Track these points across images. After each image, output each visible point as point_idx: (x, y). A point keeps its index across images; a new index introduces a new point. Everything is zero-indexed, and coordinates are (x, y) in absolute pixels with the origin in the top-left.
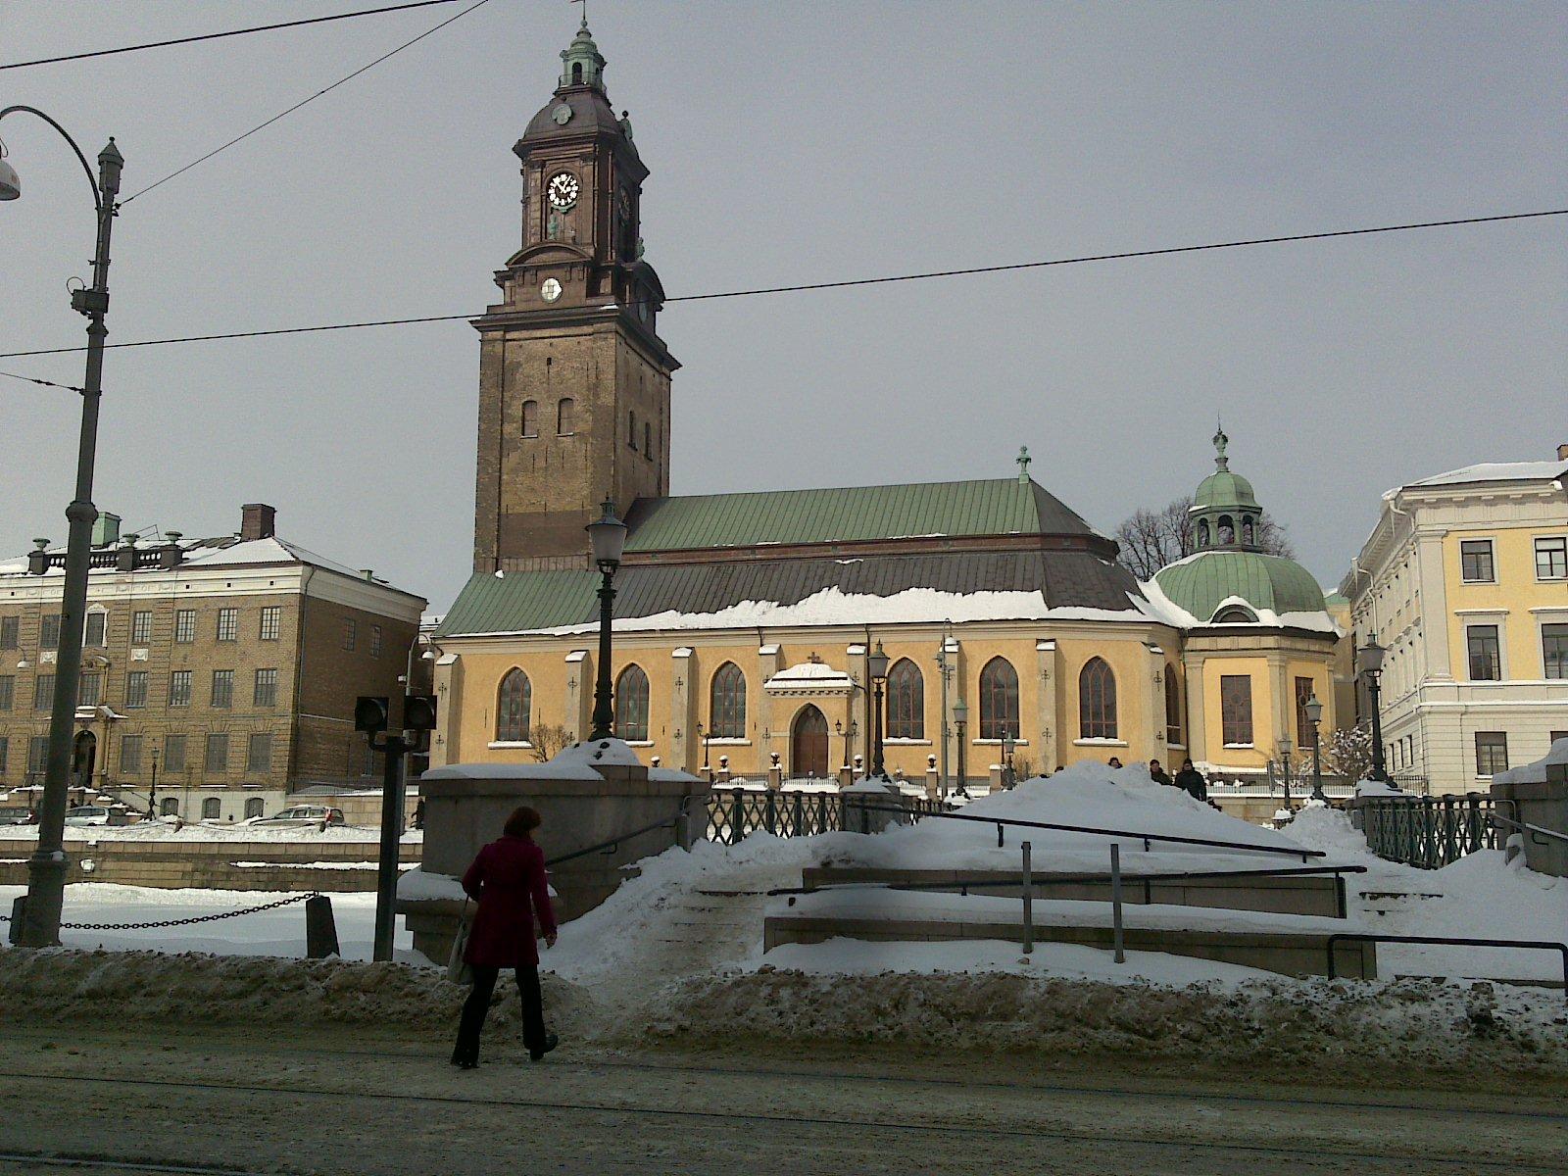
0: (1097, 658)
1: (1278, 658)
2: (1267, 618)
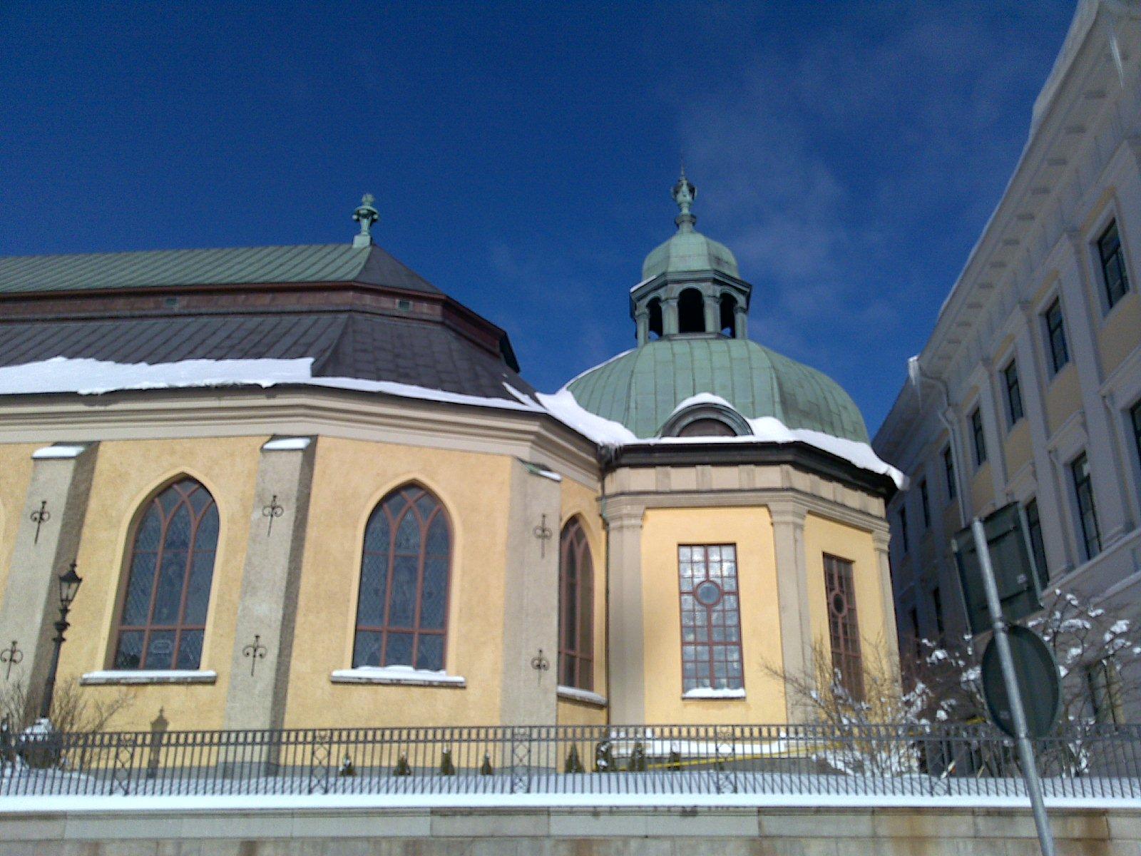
0: (413, 485)
1: (790, 506)
2: (768, 429)
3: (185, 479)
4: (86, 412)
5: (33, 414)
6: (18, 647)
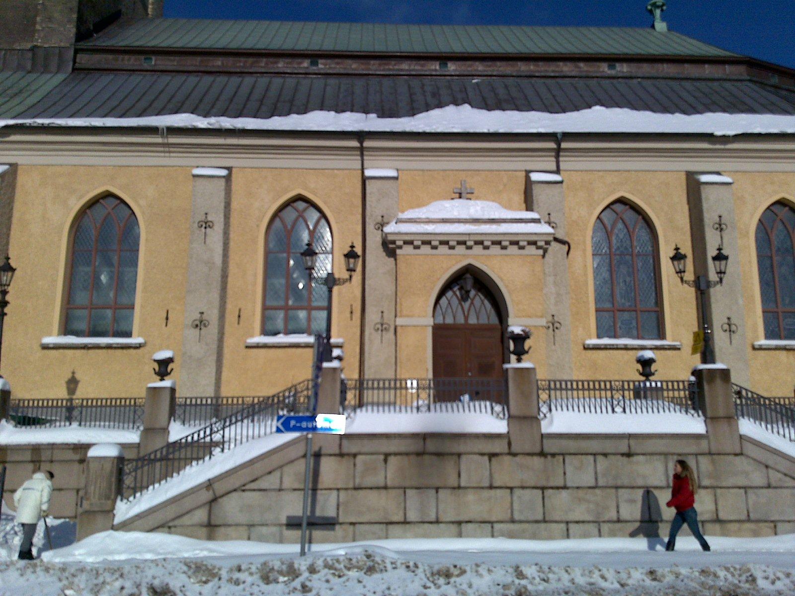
3: (108, 195)
4: (707, 149)
5: (618, 149)
6: (733, 321)
